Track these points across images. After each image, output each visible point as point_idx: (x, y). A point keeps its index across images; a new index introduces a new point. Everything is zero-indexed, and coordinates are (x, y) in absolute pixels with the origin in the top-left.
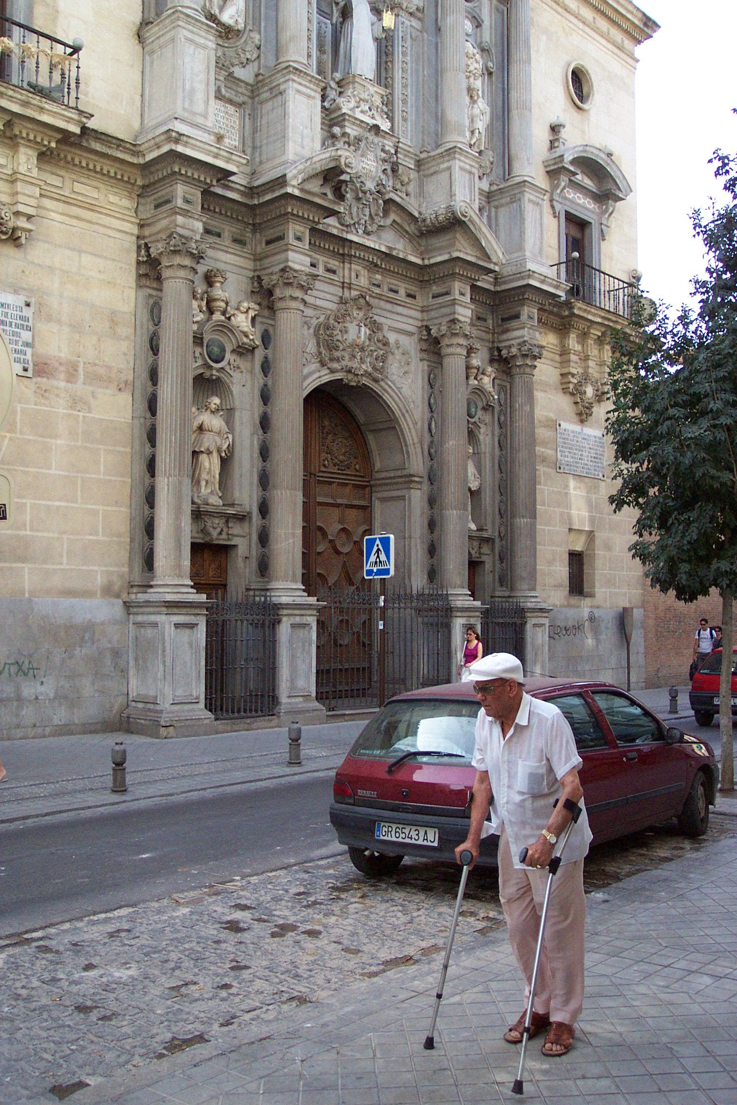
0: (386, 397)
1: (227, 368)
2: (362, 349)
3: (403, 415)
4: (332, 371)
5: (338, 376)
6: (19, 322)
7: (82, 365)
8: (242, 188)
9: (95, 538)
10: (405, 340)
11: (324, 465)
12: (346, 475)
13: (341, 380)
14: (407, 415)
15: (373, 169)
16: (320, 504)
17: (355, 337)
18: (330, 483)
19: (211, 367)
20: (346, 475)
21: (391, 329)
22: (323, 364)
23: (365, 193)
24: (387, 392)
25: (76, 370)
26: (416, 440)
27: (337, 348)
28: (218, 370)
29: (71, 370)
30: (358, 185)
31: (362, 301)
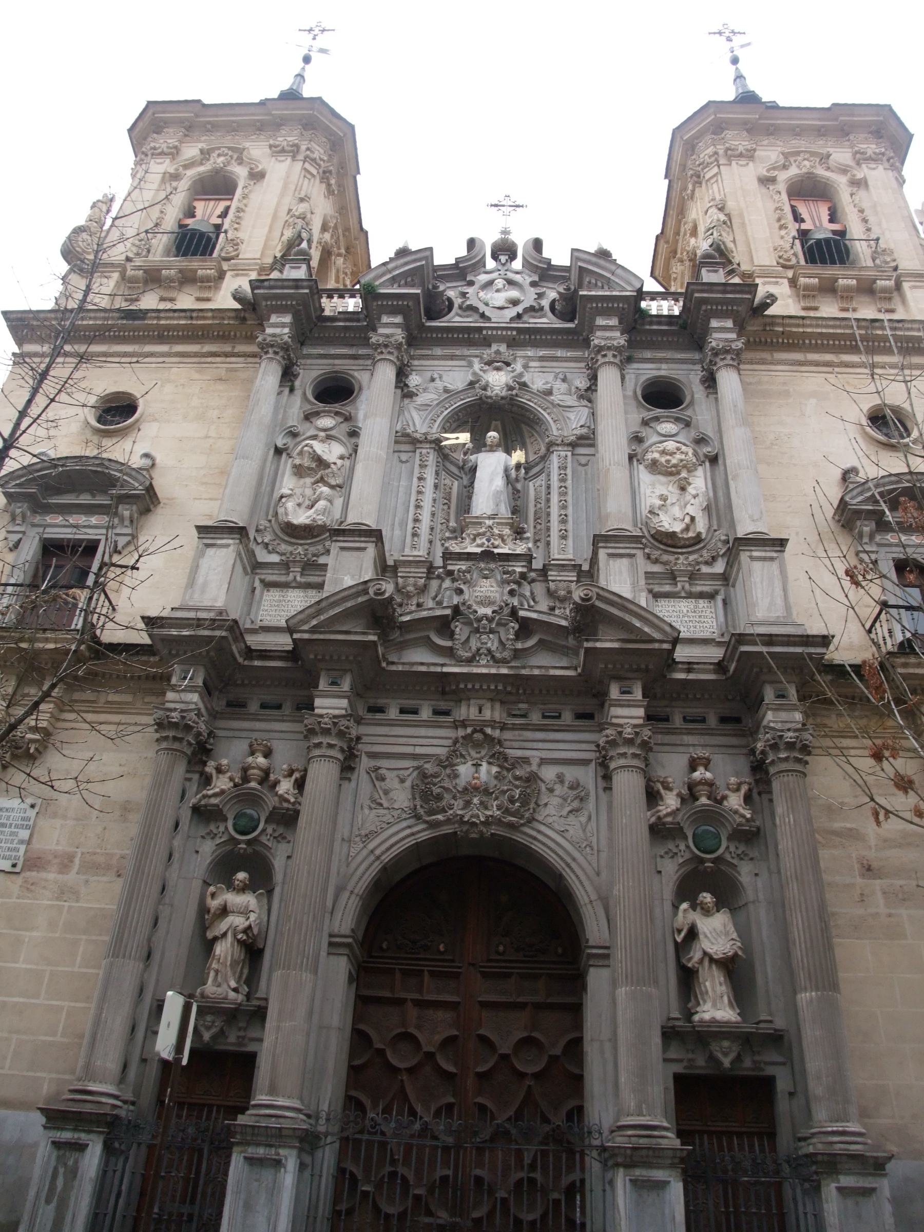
0: (536, 846)
1: (264, 839)
2: (487, 792)
3: (568, 865)
4: (437, 824)
5: (447, 830)
6: (20, 822)
7: (79, 855)
8: (284, 654)
9: (51, 1039)
10: (571, 773)
11: (498, 953)
12: (505, 961)
13: (455, 833)
14: (573, 865)
15: (497, 595)
16: (485, 1005)
17: (470, 779)
18: (507, 976)
19: (239, 842)
20: (505, 961)
21: (543, 762)
22: (418, 817)
23: (479, 620)
24: (535, 839)
25: (72, 862)
26: (594, 897)
27: (439, 798)
28: (249, 843)
29: (66, 861)
30: (472, 616)
31: (478, 736)
